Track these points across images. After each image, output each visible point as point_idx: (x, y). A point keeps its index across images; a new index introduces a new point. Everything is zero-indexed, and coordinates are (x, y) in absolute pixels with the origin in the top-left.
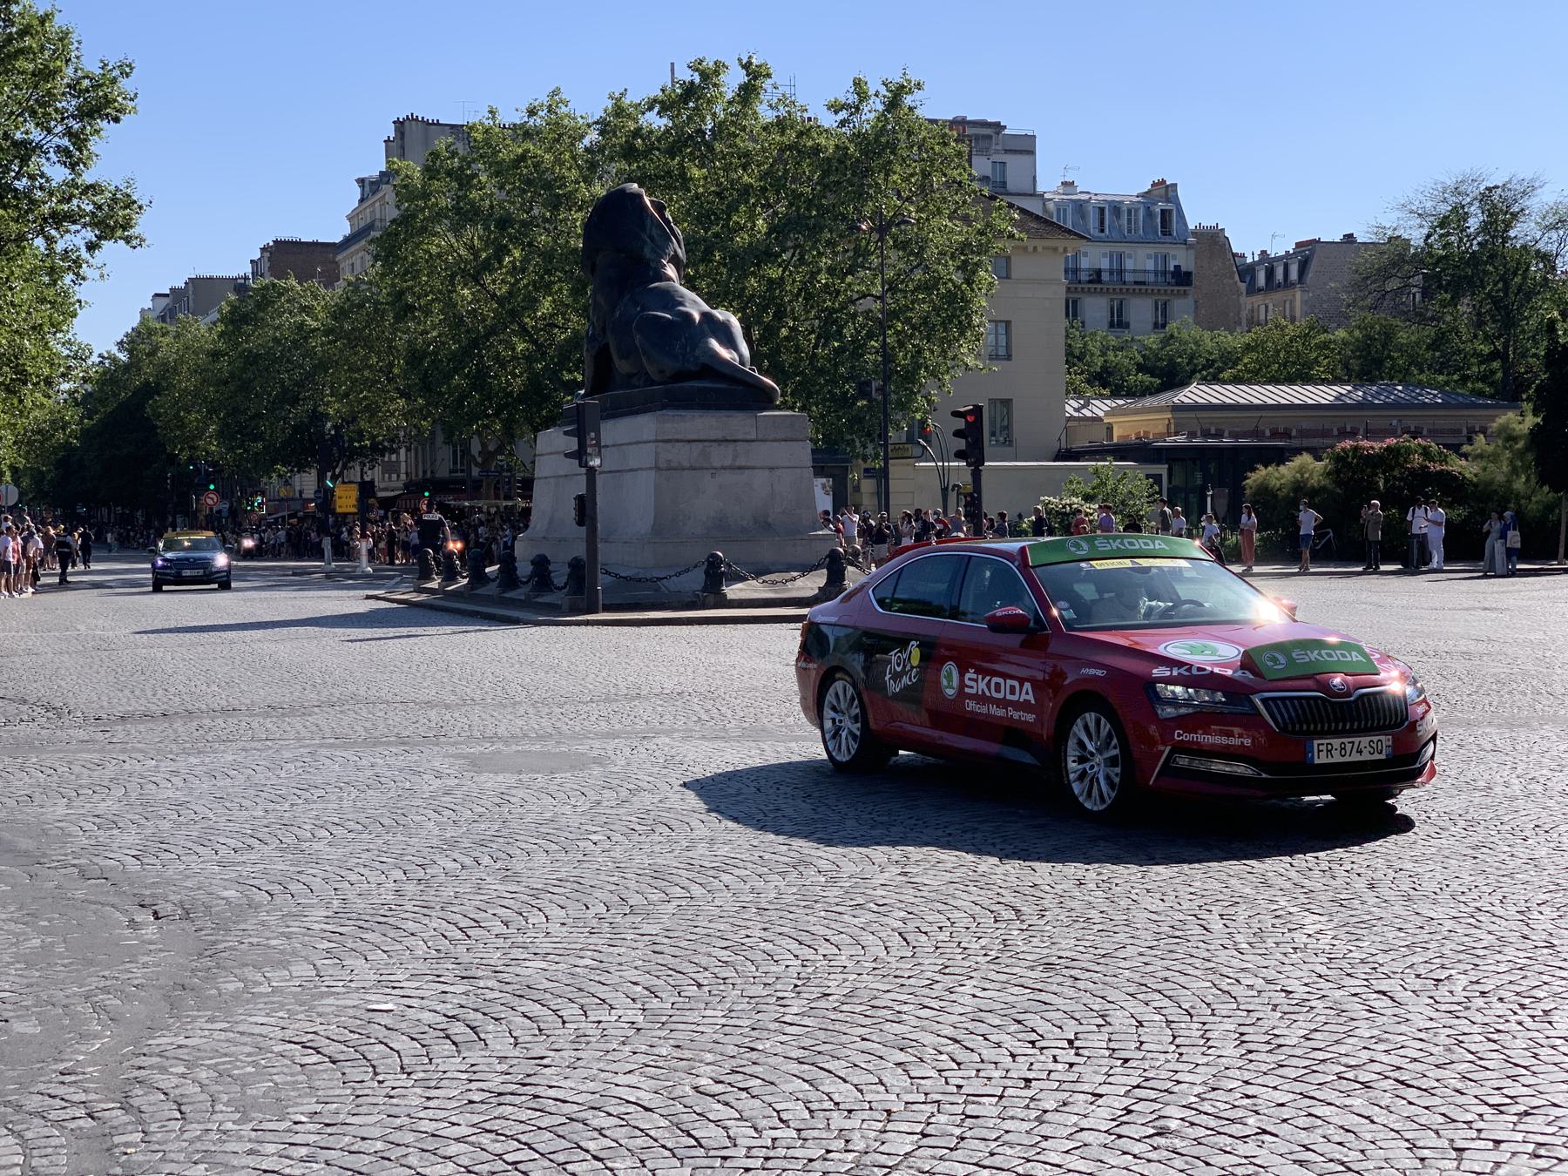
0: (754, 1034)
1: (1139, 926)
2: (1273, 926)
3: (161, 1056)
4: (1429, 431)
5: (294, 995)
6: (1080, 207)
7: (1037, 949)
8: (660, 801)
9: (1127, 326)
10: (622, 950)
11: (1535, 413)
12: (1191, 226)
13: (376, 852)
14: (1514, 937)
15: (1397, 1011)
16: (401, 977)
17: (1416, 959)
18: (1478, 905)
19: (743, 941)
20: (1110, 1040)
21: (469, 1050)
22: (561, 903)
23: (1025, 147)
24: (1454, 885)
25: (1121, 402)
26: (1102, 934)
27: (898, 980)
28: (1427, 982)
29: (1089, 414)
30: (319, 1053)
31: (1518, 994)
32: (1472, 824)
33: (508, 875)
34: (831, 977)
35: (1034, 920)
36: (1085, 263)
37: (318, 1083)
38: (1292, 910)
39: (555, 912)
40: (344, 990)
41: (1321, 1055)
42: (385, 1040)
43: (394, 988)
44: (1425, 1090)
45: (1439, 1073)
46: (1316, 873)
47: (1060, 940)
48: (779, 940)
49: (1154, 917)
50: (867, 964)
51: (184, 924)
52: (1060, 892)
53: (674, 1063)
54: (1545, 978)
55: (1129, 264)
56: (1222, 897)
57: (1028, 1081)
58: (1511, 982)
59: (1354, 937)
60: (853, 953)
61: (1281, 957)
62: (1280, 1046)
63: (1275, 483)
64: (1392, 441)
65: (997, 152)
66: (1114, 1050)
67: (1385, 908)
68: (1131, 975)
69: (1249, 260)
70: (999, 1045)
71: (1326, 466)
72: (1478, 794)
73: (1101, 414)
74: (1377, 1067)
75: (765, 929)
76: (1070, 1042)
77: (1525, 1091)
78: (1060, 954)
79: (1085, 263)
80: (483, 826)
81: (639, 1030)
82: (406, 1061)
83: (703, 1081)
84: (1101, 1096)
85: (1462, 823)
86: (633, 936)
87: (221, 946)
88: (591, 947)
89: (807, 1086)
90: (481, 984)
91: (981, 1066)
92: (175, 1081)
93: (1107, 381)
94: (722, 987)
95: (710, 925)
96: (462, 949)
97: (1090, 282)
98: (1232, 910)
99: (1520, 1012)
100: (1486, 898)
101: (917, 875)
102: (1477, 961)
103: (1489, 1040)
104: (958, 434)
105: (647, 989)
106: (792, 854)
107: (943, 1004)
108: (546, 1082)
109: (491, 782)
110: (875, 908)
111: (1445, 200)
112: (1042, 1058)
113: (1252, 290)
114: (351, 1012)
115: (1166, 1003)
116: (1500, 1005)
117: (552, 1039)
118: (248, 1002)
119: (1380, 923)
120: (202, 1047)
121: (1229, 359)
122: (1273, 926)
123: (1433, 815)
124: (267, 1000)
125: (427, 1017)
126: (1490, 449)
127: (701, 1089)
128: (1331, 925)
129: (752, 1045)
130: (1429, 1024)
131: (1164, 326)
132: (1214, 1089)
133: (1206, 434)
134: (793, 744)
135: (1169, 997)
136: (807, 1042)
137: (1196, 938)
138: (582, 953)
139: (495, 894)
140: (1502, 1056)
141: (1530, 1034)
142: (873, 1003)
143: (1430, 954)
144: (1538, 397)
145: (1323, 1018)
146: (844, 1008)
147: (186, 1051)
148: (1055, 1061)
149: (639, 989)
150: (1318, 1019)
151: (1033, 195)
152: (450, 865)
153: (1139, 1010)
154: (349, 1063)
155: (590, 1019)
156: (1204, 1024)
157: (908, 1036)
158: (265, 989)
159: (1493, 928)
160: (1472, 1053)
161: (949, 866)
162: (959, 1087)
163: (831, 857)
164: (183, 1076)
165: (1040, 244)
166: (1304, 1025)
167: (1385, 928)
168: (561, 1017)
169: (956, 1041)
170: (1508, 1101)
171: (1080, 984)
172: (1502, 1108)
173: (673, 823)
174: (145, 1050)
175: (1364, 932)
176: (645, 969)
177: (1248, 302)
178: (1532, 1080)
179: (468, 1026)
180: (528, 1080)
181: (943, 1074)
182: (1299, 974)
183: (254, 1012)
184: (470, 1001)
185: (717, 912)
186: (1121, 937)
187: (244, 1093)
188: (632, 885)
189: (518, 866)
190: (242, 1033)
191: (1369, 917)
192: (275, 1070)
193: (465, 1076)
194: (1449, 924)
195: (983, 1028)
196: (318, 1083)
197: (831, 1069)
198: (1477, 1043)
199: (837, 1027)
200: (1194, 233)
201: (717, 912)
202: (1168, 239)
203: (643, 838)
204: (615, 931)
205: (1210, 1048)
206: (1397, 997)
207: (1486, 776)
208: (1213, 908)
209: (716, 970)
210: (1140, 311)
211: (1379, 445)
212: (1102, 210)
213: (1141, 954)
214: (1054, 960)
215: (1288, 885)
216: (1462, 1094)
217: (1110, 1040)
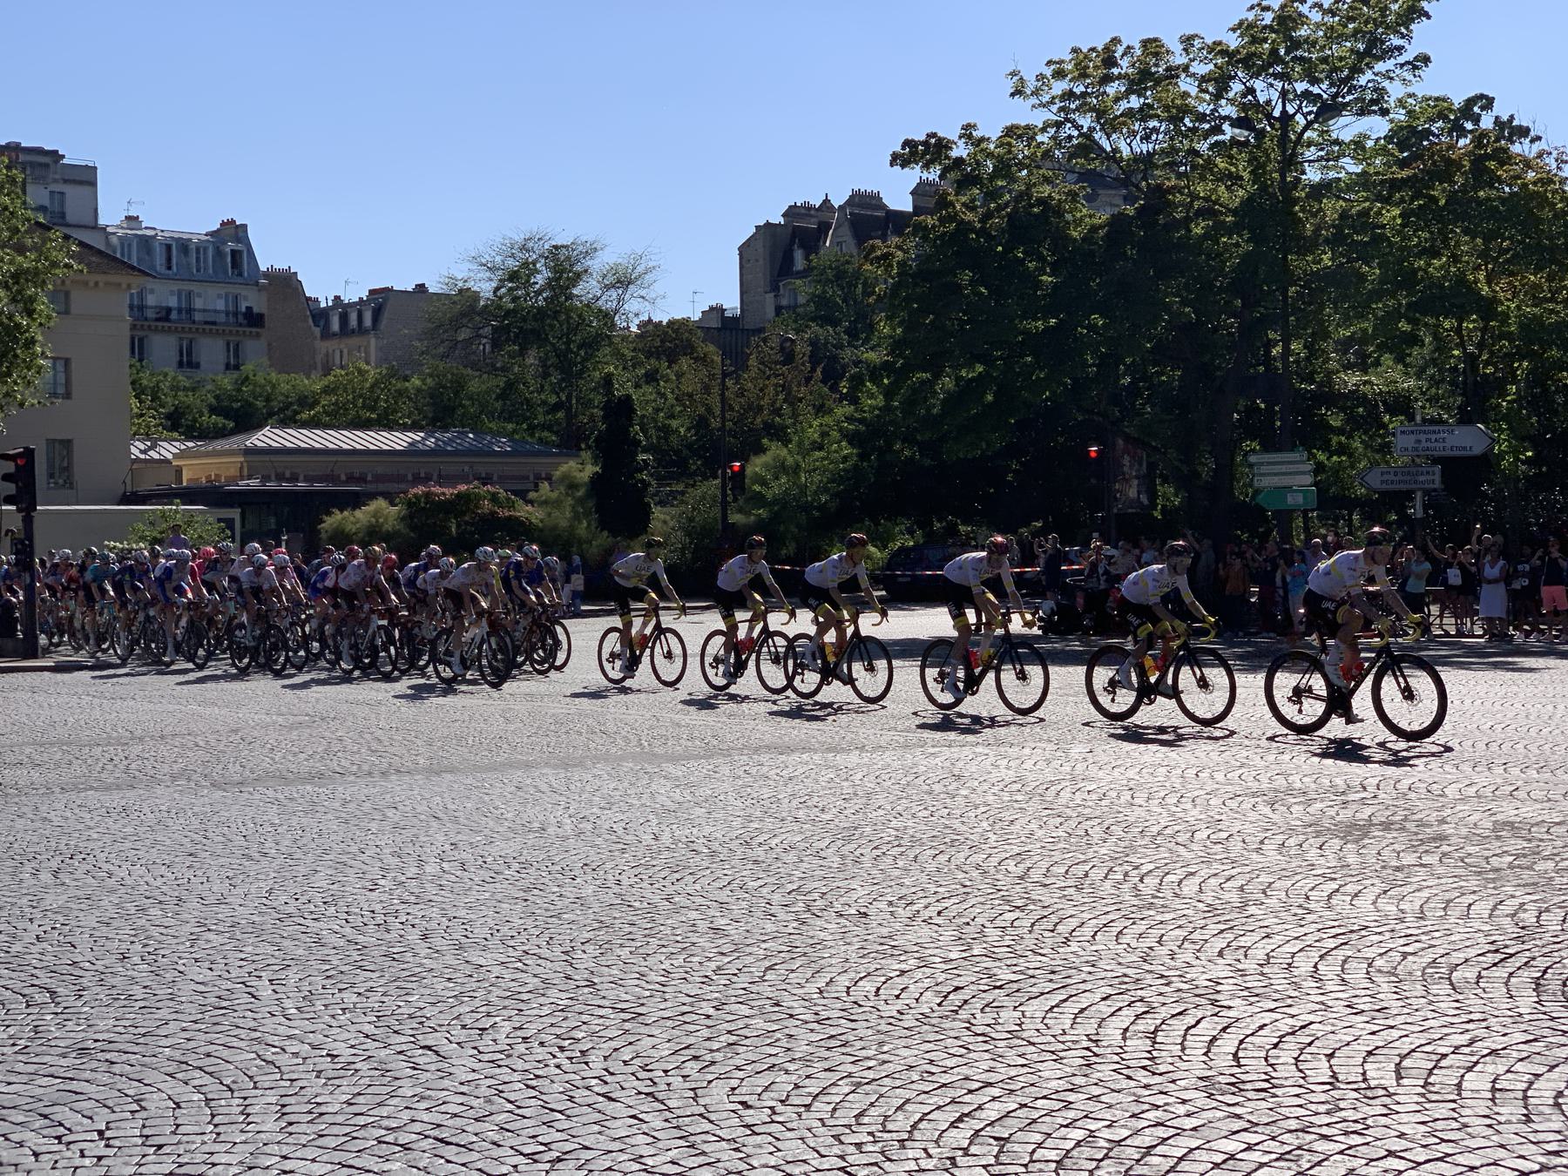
1: (183, 999)
4: (500, 477)
6: (146, 243)
7: (76, 1031)
9: (197, 366)
11: (594, 464)
12: (263, 268)
14: (557, 979)
17: (464, 1009)
20: (144, 1126)
23: (86, 177)
24: (505, 930)
25: (190, 444)
26: (144, 1011)
28: (473, 1032)
29: (156, 456)
31: (558, 1036)
32: (524, 866)
35: (71, 1001)
36: (151, 300)
41: (362, 1120)
45: (478, 1127)
47: (98, 1022)
49: (201, 988)
52: (101, 969)
54: (585, 1018)
55: (198, 303)
58: (552, 1025)
61: (327, 1019)
62: (322, 1114)
63: (350, 528)
64: (463, 488)
65: (55, 181)
66: (147, 1137)
67: (436, 958)
68: (172, 1054)
69: (323, 305)
70: (21, 1144)
71: (400, 512)
73: (170, 456)
74: (417, 1127)
76: (101, 1133)
77: (559, 1136)
79: (151, 300)
85: (516, 866)
93: (178, 423)
97: (157, 320)
99: (559, 1055)
100: (534, 940)
102: (522, 1006)
103: (528, 1086)
104: (7, 477)
111: (513, 256)
112: (69, 1154)
113: (327, 334)
115: (207, 1079)
116: (540, 1050)
119: (430, 975)
121: (306, 401)
122: (324, 987)
123: (489, 860)
126: (554, 495)
128: (383, 981)
131: (237, 367)
133: (280, 478)
137: (243, 1007)
140: (540, 1102)
141: (567, 1077)
143: (477, 1003)
144: (597, 447)
145: (367, 1081)
148: (83, 1156)
150: (362, 1082)
151: (95, 227)
156: (245, 1098)
159: (539, 970)
160: (511, 1102)
165: (101, 278)
166: (347, 1090)
167: (435, 980)
170: (542, 1148)
172: (536, 1157)
175: (414, 985)
177: (323, 347)
178: (566, 1125)
182: (346, 1035)
191: (420, 970)
194: (497, 970)
198: (517, 1092)
200: (266, 275)
202: (240, 280)
205: (249, 1124)
206: (442, 1050)
207: (541, 818)
208: (263, 974)
210: (211, 351)
211: (450, 492)
212: (169, 247)
213: (184, 1030)
214: (90, 1044)
215: (342, 942)
216: (499, 1146)
217: (144, 1126)
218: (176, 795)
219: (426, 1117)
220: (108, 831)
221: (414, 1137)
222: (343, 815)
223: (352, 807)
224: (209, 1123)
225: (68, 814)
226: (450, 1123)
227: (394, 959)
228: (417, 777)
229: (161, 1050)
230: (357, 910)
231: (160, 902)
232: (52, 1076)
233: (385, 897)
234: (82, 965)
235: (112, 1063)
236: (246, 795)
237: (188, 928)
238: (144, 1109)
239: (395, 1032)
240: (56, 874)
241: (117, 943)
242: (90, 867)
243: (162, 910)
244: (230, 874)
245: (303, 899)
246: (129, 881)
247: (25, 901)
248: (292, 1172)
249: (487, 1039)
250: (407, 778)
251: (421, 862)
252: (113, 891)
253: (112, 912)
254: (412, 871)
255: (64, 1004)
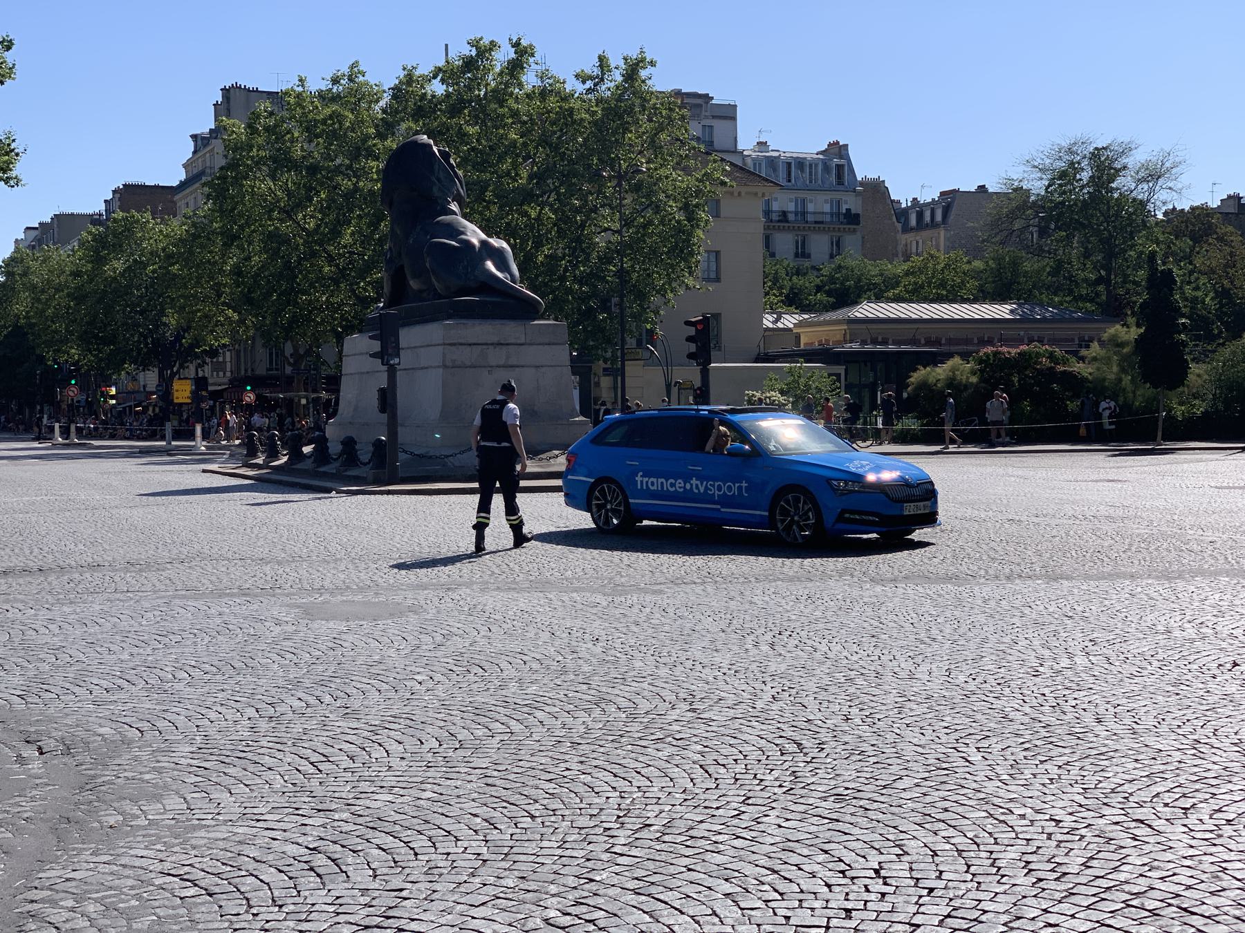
0: (589, 864)
1: (908, 758)
2: (1025, 758)
3: (51, 890)
5: (169, 827)
8: (471, 645)
10: (459, 783)
13: (230, 692)
15: (1159, 839)
16: (264, 810)
18: (1196, 737)
19: (564, 773)
20: (911, 869)
21: (332, 882)
22: (398, 738)
24: (1169, 718)
26: (879, 766)
27: (707, 811)
28: (1176, 810)
30: (196, 885)
33: (348, 713)
34: (649, 808)
35: (815, 752)
37: (198, 916)
38: (1039, 743)
39: (394, 747)
40: (213, 823)
42: (255, 873)
43: (258, 821)
44: (1208, 917)
46: (1046, 709)
48: (594, 771)
49: (920, 750)
50: (677, 796)
51: (66, 759)
53: (522, 895)
56: (972, 731)
57: (848, 911)
59: (1098, 769)
60: (664, 785)
61: (1041, 787)
62: (1065, 874)
66: (918, 879)
72: (1161, 637)
75: (581, 762)
76: (876, 871)
78: (846, 785)
80: (321, 668)
81: (485, 861)
82: (276, 893)
83: (552, 913)
84: (918, 926)
85: (1156, 664)
86: (466, 770)
87: (100, 780)
88: (430, 780)
89: (647, 918)
90: (336, 817)
91: (801, 896)
92: (67, 915)
94: (553, 819)
95: (533, 759)
96: (314, 782)
98: (985, 744)
100: (1199, 730)
101: (704, 711)
105: (486, 820)
106: (592, 692)
107: (754, 834)
108: (407, 915)
109: (321, 626)
110: (675, 743)
112: (855, 888)
114: (221, 844)
115: (951, 832)
117: (407, 871)
118: (127, 834)
119: (1117, 755)
120: (88, 880)
122: (1025, 758)
124: (144, 832)
125: (291, 849)
127: (551, 921)
129: (590, 876)
130: (1191, 852)
132: (1018, 918)
134: (575, 595)
135: (954, 827)
136: (640, 873)
137: (962, 770)
138: (423, 787)
139: (339, 730)
142: (691, 833)
146: (666, 838)
147: (74, 883)
149: (478, 820)
150: (1091, 846)
152: (297, 704)
153: (930, 839)
154: (224, 896)
155: (439, 851)
156: (991, 852)
157: (729, 866)
158: (142, 822)
159: (1216, 759)
161: (730, 703)
162: (787, 918)
163: (626, 695)
164: (72, 910)
167: (1124, 760)
168: (412, 849)
169: (775, 872)
171: (871, 814)
173: (484, 664)
174: (36, 883)
176: (481, 801)
179: (329, 858)
180: (390, 913)
181: (769, 904)
182: (1061, 804)
183: (134, 845)
184: (329, 834)
185: (537, 746)
186: (894, 769)
187: (130, 927)
188: (457, 720)
189: (356, 704)
190: (124, 866)
191: (1104, 750)
192: (156, 904)
193: (332, 909)
194: (1177, 755)
195: (795, 859)
196: (198, 916)
197: (666, 899)
199: (663, 857)
201: (537, 746)
203: (460, 678)
204: (449, 765)
205: (1003, 876)
206: (1154, 824)
208: (967, 742)
209: (545, 802)
213: (917, 785)
214: (841, 791)
218: (846, 587)
219: (1163, 886)
220: (801, 614)
221: (1159, 904)
222: (987, 610)
223: (992, 603)
224: (966, 872)
225: (767, 598)
226: (1187, 893)
227: (1079, 738)
228: (1040, 582)
229: (905, 802)
230: (1029, 692)
231: (862, 674)
232: (820, 816)
233: (1050, 683)
234: (816, 722)
235: (866, 809)
236: (901, 591)
237: (890, 699)
238: (906, 853)
239: (1105, 804)
240: (772, 645)
241: (838, 707)
242: (796, 642)
243: (865, 680)
244: (911, 654)
245: (979, 679)
246: (830, 655)
247: (754, 666)
248: (1057, 925)
249: (1192, 820)
250: (1029, 582)
251: (1071, 656)
252: (821, 663)
253: (826, 680)
254: (1065, 662)
255: (811, 755)
